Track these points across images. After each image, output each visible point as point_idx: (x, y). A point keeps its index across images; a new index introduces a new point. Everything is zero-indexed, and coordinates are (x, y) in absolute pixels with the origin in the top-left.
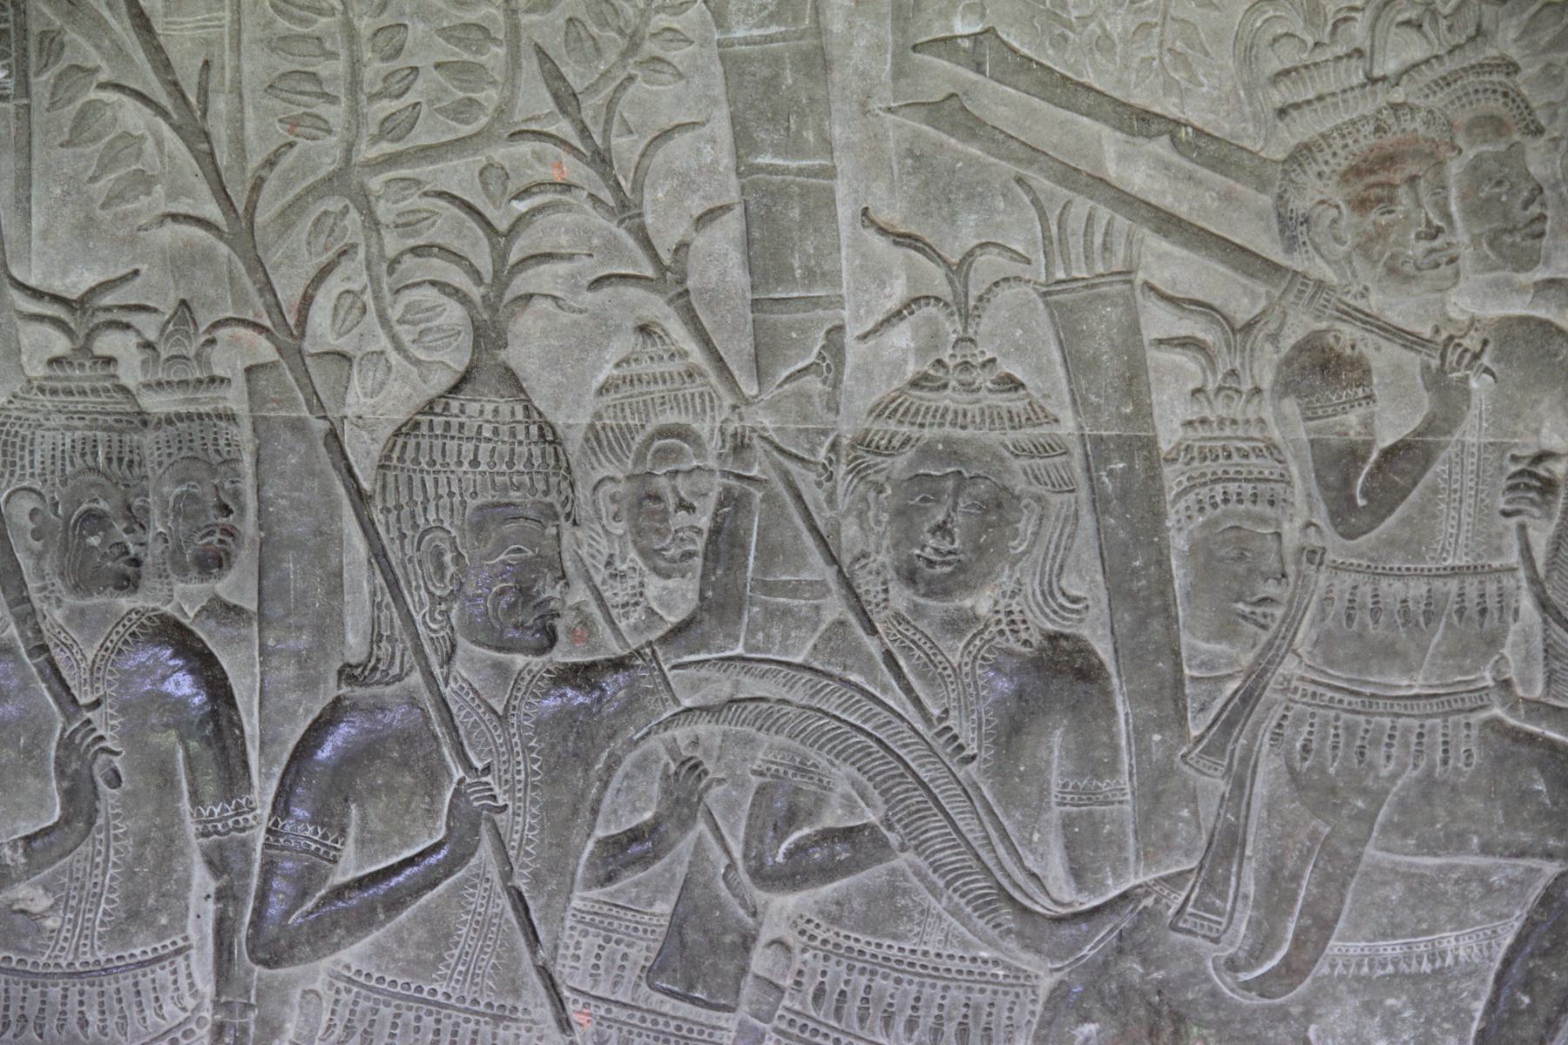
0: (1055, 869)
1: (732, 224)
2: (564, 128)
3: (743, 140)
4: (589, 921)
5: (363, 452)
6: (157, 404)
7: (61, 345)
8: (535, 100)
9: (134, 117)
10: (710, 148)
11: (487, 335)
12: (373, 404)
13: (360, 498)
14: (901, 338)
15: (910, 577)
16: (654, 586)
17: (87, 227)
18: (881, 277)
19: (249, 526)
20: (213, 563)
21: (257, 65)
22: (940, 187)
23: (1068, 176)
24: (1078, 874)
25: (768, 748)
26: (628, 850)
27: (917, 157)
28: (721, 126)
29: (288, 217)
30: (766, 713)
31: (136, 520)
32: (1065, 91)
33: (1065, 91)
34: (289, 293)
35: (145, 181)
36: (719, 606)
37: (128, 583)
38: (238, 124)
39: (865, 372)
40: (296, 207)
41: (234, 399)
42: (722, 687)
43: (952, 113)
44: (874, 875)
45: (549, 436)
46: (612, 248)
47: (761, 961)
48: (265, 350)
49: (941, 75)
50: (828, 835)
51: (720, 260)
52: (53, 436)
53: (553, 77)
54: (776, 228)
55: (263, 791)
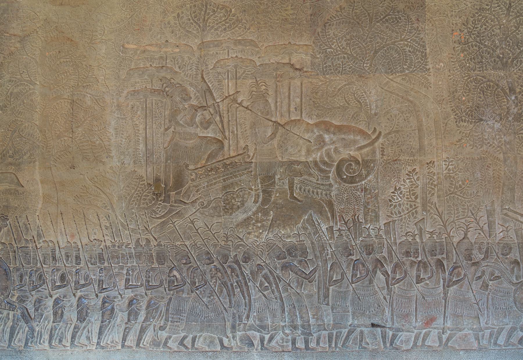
0: (514, 279)
1: (487, 224)
2: (472, 216)
3: (488, 217)
4: (475, 284)
5: (455, 244)
6: (437, 241)
7: (430, 236)
8: (470, 214)
9: (436, 216)
10: (485, 218)
11: (466, 234)
12: (456, 240)
13: (455, 249)
14: (501, 234)
15: (503, 254)
16: (480, 255)
17: (432, 226)
18: (500, 229)
19: (445, 251)
20: (443, 254)
21: (446, 212)
22: (505, 221)
23: (516, 220)
24: (517, 279)
25: (491, 269)
26: (479, 278)
27: (503, 219)
28: (486, 216)
29: (449, 225)
30: (490, 266)
31: (436, 251)
32: (516, 213)
33: (516, 213)
34: (449, 231)
35: (437, 222)
36: (486, 258)
37: (435, 256)
38: (444, 217)
39: (498, 237)
40: (450, 223)
41: (444, 240)
42: (486, 264)
43: (506, 214)
44: (500, 280)
45: (471, 243)
46: (477, 227)
47: (489, 287)
48: (447, 236)
49: (505, 211)
50: (496, 276)
51: (486, 227)
52: (429, 243)
53: (472, 212)
54: (491, 225)
55: (447, 273)
